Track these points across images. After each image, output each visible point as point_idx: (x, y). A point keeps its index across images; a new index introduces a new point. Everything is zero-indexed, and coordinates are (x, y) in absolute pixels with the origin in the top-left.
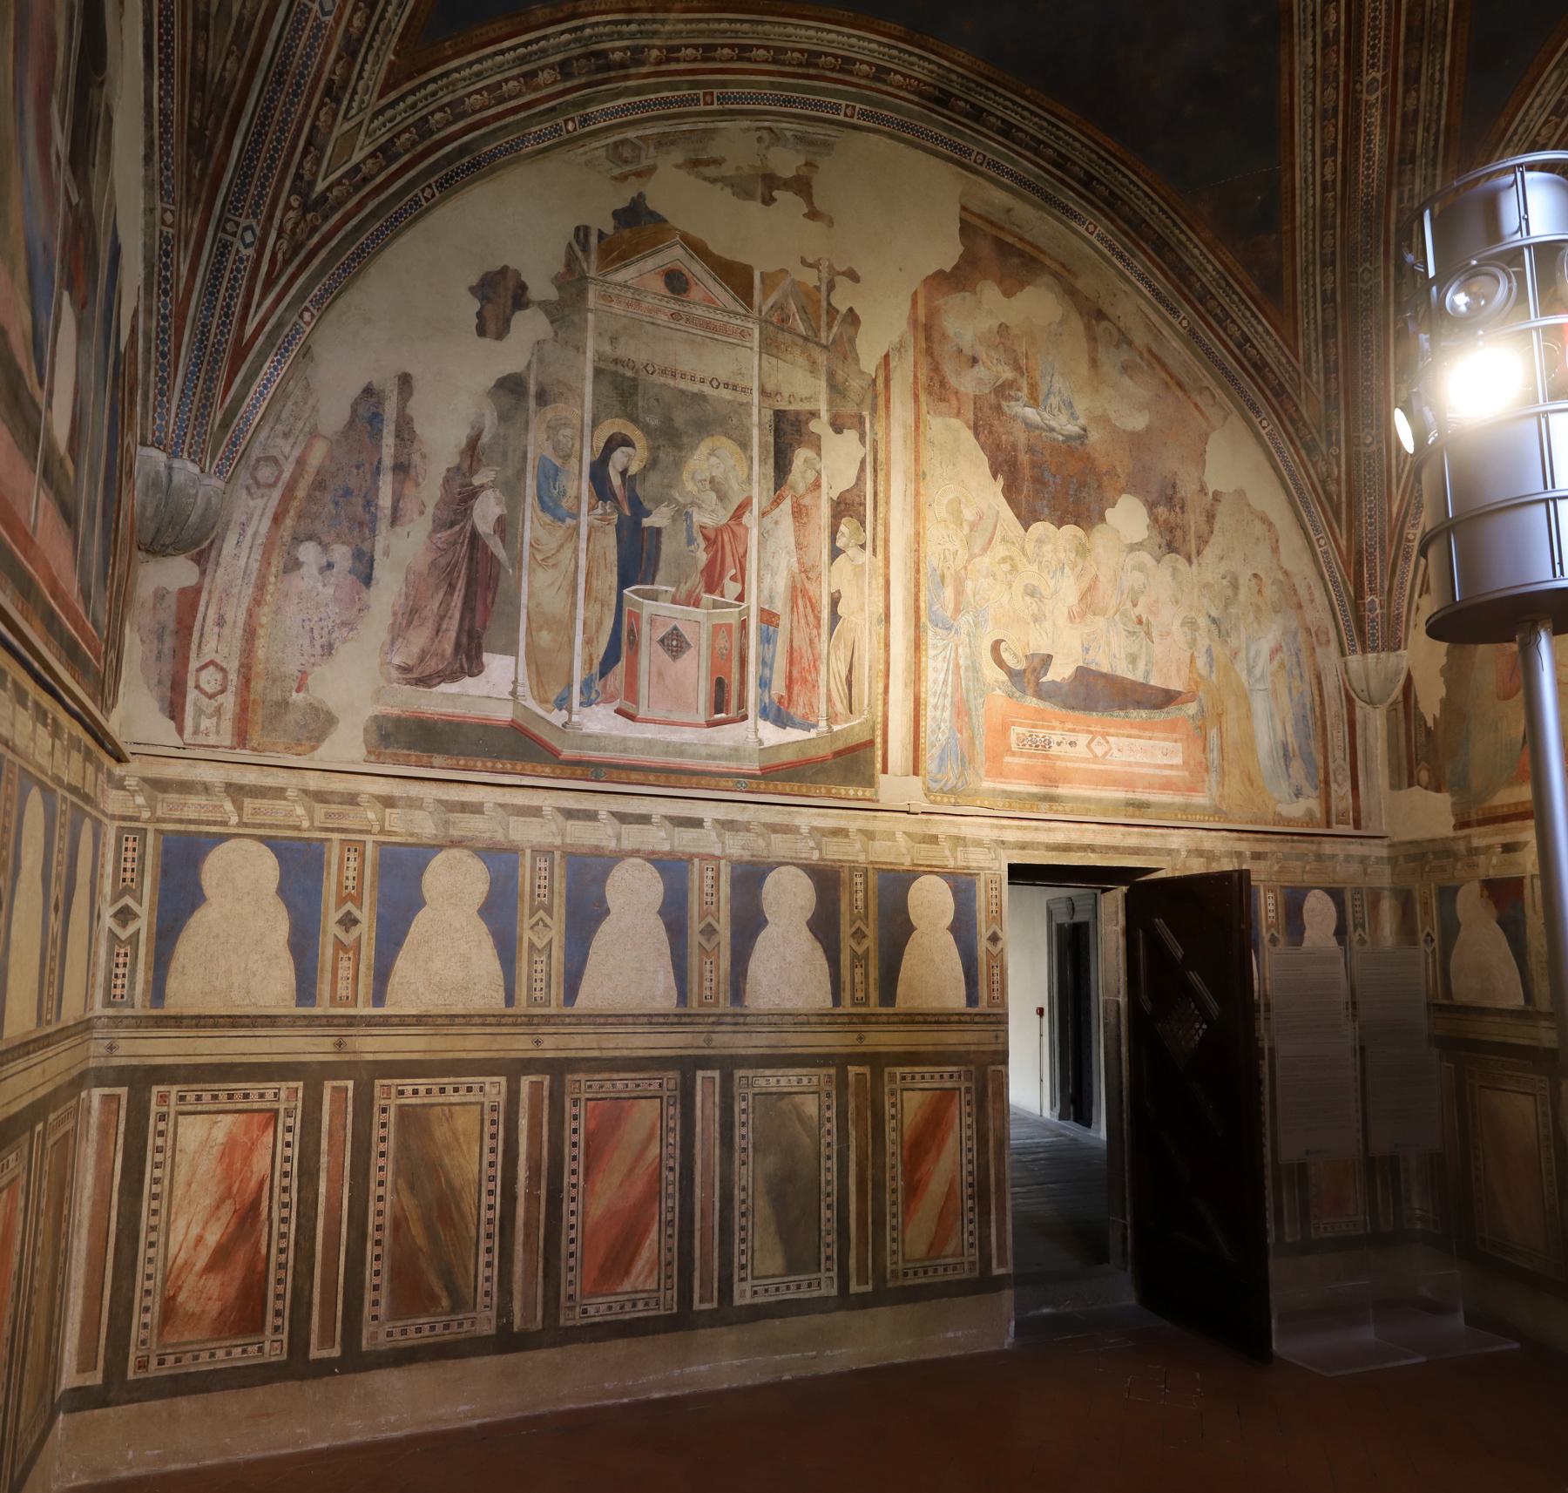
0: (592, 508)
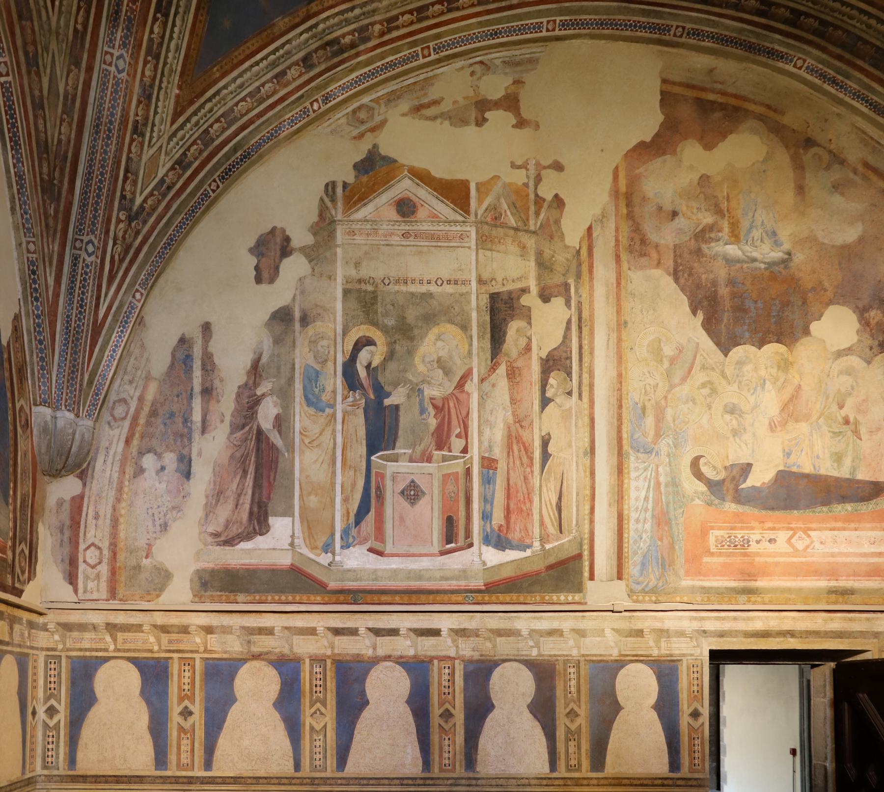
0: (345, 398)
